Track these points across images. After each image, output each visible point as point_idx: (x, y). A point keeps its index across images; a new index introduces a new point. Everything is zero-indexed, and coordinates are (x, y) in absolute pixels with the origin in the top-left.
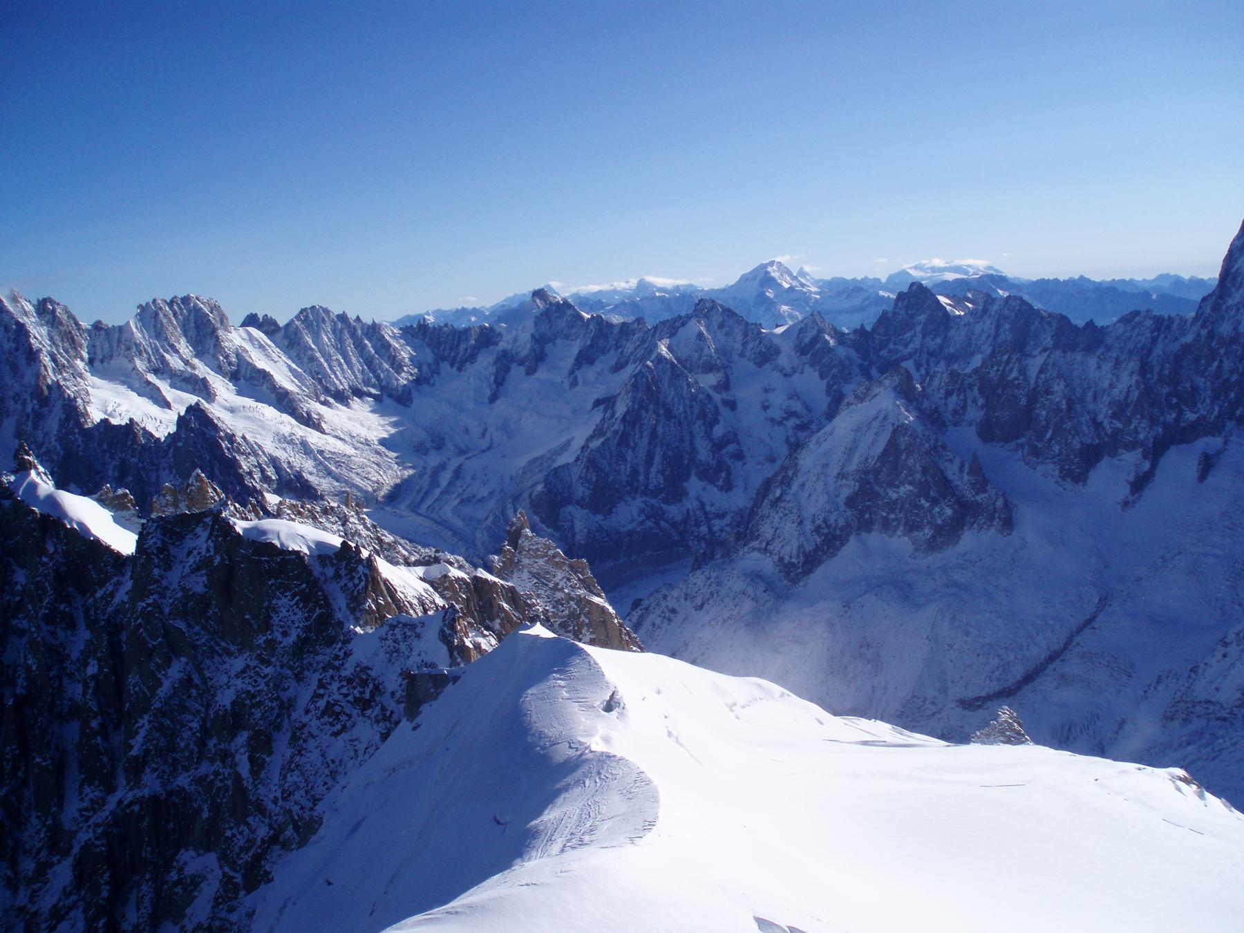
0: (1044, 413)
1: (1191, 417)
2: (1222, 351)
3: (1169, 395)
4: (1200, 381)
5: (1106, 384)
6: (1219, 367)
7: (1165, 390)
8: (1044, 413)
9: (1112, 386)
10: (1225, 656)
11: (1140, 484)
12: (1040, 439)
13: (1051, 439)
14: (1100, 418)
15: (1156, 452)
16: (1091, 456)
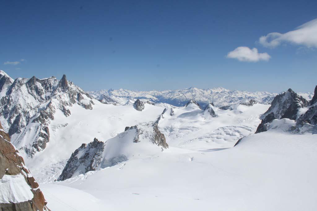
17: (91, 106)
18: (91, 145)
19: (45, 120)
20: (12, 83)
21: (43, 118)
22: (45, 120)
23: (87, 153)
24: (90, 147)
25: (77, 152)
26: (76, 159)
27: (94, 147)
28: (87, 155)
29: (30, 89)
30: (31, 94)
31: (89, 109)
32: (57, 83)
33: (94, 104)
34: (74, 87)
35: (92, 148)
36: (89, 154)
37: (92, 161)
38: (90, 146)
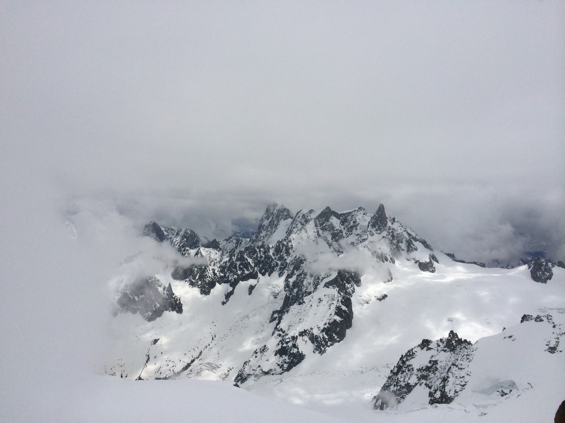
0: (196, 269)
1: (246, 272)
2: (258, 250)
3: (240, 265)
4: (250, 260)
5: (218, 260)
6: (257, 256)
7: (238, 263)
8: (196, 269)
9: (221, 261)
10: (256, 357)
11: (228, 295)
12: (194, 278)
13: (198, 278)
14: (216, 272)
15: (234, 284)
16: (212, 285)
17: (432, 265)
18: (441, 344)
19: (346, 284)
20: (292, 218)
21: (343, 281)
22: (346, 284)
23: (433, 359)
24: (439, 348)
25: (410, 354)
26: (410, 368)
27: (448, 350)
28: (433, 364)
29: (321, 229)
30: (328, 243)
31: (428, 270)
32: (368, 219)
33: (437, 262)
34: (399, 228)
35: (445, 351)
36: (437, 364)
37: (445, 380)
38: (439, 346)
